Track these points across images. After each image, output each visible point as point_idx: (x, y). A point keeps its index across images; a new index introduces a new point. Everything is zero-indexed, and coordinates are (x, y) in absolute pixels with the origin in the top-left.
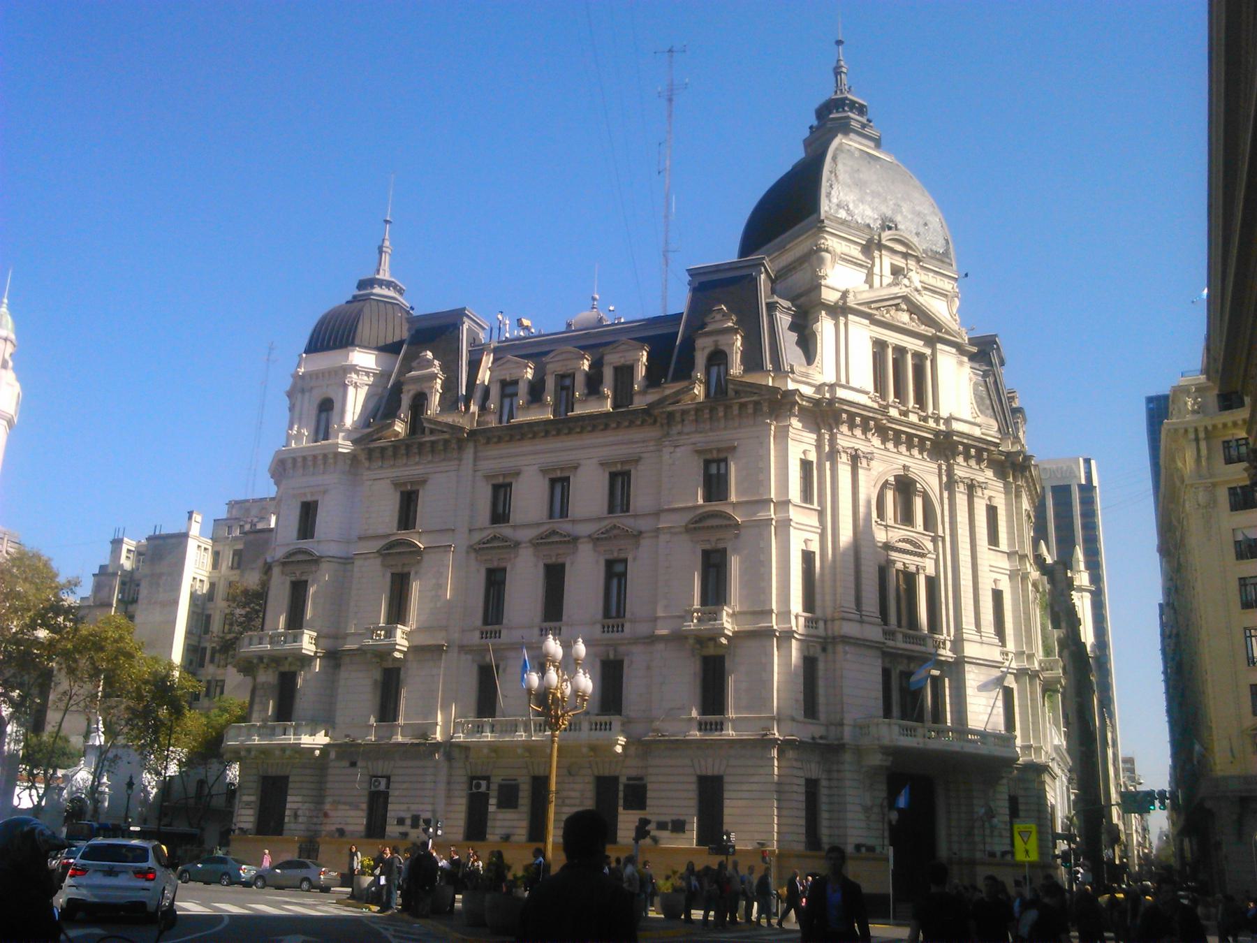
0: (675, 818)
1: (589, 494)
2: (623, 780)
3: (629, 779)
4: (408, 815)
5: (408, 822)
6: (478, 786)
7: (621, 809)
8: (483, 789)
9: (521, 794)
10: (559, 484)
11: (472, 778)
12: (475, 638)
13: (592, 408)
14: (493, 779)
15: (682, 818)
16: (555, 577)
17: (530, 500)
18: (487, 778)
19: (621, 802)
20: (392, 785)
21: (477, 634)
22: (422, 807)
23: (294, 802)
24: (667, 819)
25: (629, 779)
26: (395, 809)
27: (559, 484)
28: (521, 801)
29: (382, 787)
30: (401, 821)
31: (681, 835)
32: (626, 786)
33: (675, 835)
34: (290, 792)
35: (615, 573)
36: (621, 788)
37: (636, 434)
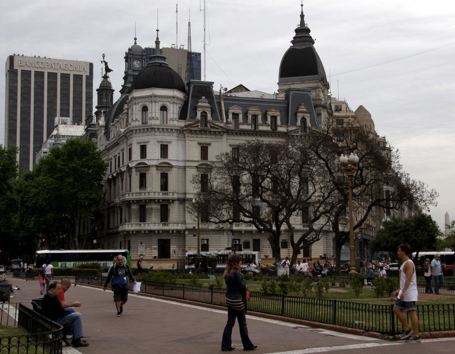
6: (236, 242)
8: (237, 242)
11: (234, 240)
14: (241, 240)
18: (239, 240)
20: (209, 242)
22: (221, 248)
23: (173, 248)
28: (251, 246)
29: (206, 242)
32: (282, 242)
34: (171, 244)
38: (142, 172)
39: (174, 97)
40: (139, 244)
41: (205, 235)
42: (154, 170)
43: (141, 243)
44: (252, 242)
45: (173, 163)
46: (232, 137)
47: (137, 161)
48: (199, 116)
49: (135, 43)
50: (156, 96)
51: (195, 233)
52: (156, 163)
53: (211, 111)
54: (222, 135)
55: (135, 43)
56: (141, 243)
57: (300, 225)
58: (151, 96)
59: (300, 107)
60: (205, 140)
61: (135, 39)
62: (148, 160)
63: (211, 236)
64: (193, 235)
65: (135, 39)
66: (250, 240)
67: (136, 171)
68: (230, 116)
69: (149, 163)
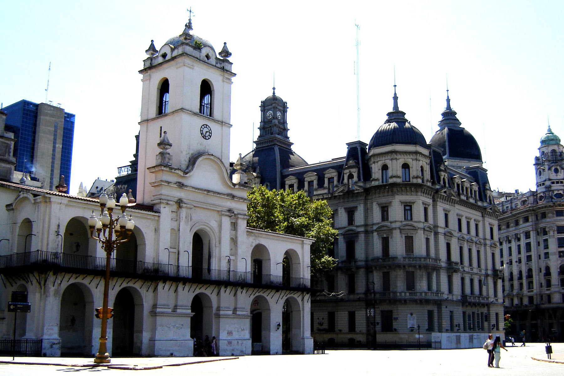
4: (457, 324)
30: (456, 325)
38: (409, 235)
40: (409, 315)
42: (421, 232)
43: (412, 314)
47: (401, 222)
48: (442, 182)
49: (274, 93)
50: (420, 153)
52: (421, 225)
55: (274, 93)
56: (412, 314)
58: (417, 153)
60: (447, 207)
61: (274, 89)
62: (416, 222)
65: (274, 89)
67: (401, 232)
69: (394, 225)
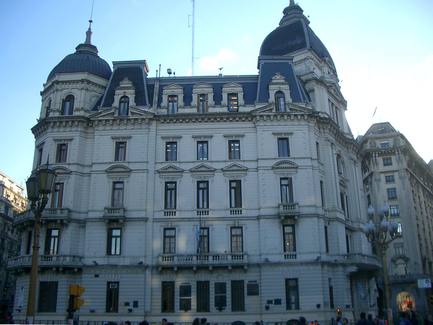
0: (276, 298)
1: (218, 149)
2: (246, 282)
3: (249, 282)
5: (131, 304)
7: (246, 295)
9: (192, 290)
10: (203, 142)
12: (161, 215)
13: (218, 110)
15: (279, 298)
16: (203, 188)
17: (187, 150)
19: (246, 292)
20: (120, 286)
21: (163, 213)
24: (272, 299)
25: (249, 282)
26: (122, 299)
27: (203, 142)
30: (127, 304)
31: (279, 306)
33: (276, 306)
35: (236, 188)
36: (245, 285)
37: (240, 124)
39: (82, 81)
41: (113, 276)
44: (196, 286)
45: (72, 168)
46: (166, 126)
51: (97, 272)
53: (136, 93)
54: (149, 124)
57: (280, 254)
59: (273, 78)
60: (121, 131)
63: (123, 276)
64: (94, 276)
66: (191, 283)
68: (165, 98)
